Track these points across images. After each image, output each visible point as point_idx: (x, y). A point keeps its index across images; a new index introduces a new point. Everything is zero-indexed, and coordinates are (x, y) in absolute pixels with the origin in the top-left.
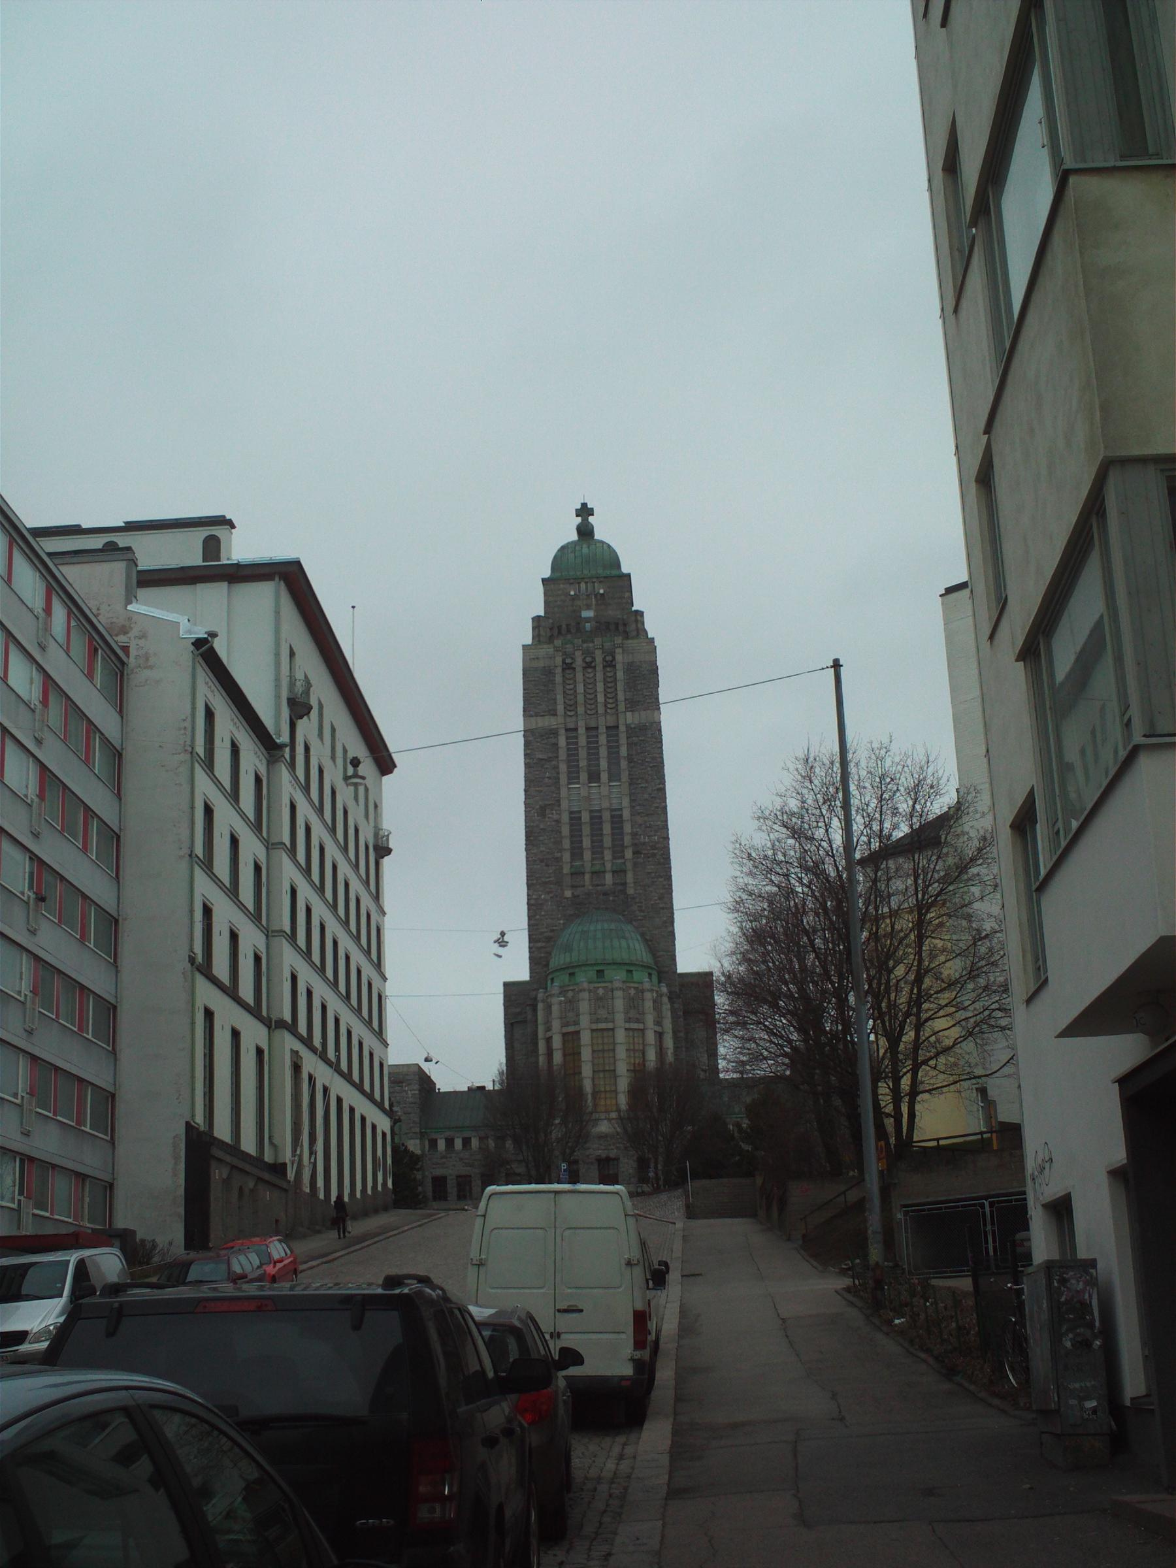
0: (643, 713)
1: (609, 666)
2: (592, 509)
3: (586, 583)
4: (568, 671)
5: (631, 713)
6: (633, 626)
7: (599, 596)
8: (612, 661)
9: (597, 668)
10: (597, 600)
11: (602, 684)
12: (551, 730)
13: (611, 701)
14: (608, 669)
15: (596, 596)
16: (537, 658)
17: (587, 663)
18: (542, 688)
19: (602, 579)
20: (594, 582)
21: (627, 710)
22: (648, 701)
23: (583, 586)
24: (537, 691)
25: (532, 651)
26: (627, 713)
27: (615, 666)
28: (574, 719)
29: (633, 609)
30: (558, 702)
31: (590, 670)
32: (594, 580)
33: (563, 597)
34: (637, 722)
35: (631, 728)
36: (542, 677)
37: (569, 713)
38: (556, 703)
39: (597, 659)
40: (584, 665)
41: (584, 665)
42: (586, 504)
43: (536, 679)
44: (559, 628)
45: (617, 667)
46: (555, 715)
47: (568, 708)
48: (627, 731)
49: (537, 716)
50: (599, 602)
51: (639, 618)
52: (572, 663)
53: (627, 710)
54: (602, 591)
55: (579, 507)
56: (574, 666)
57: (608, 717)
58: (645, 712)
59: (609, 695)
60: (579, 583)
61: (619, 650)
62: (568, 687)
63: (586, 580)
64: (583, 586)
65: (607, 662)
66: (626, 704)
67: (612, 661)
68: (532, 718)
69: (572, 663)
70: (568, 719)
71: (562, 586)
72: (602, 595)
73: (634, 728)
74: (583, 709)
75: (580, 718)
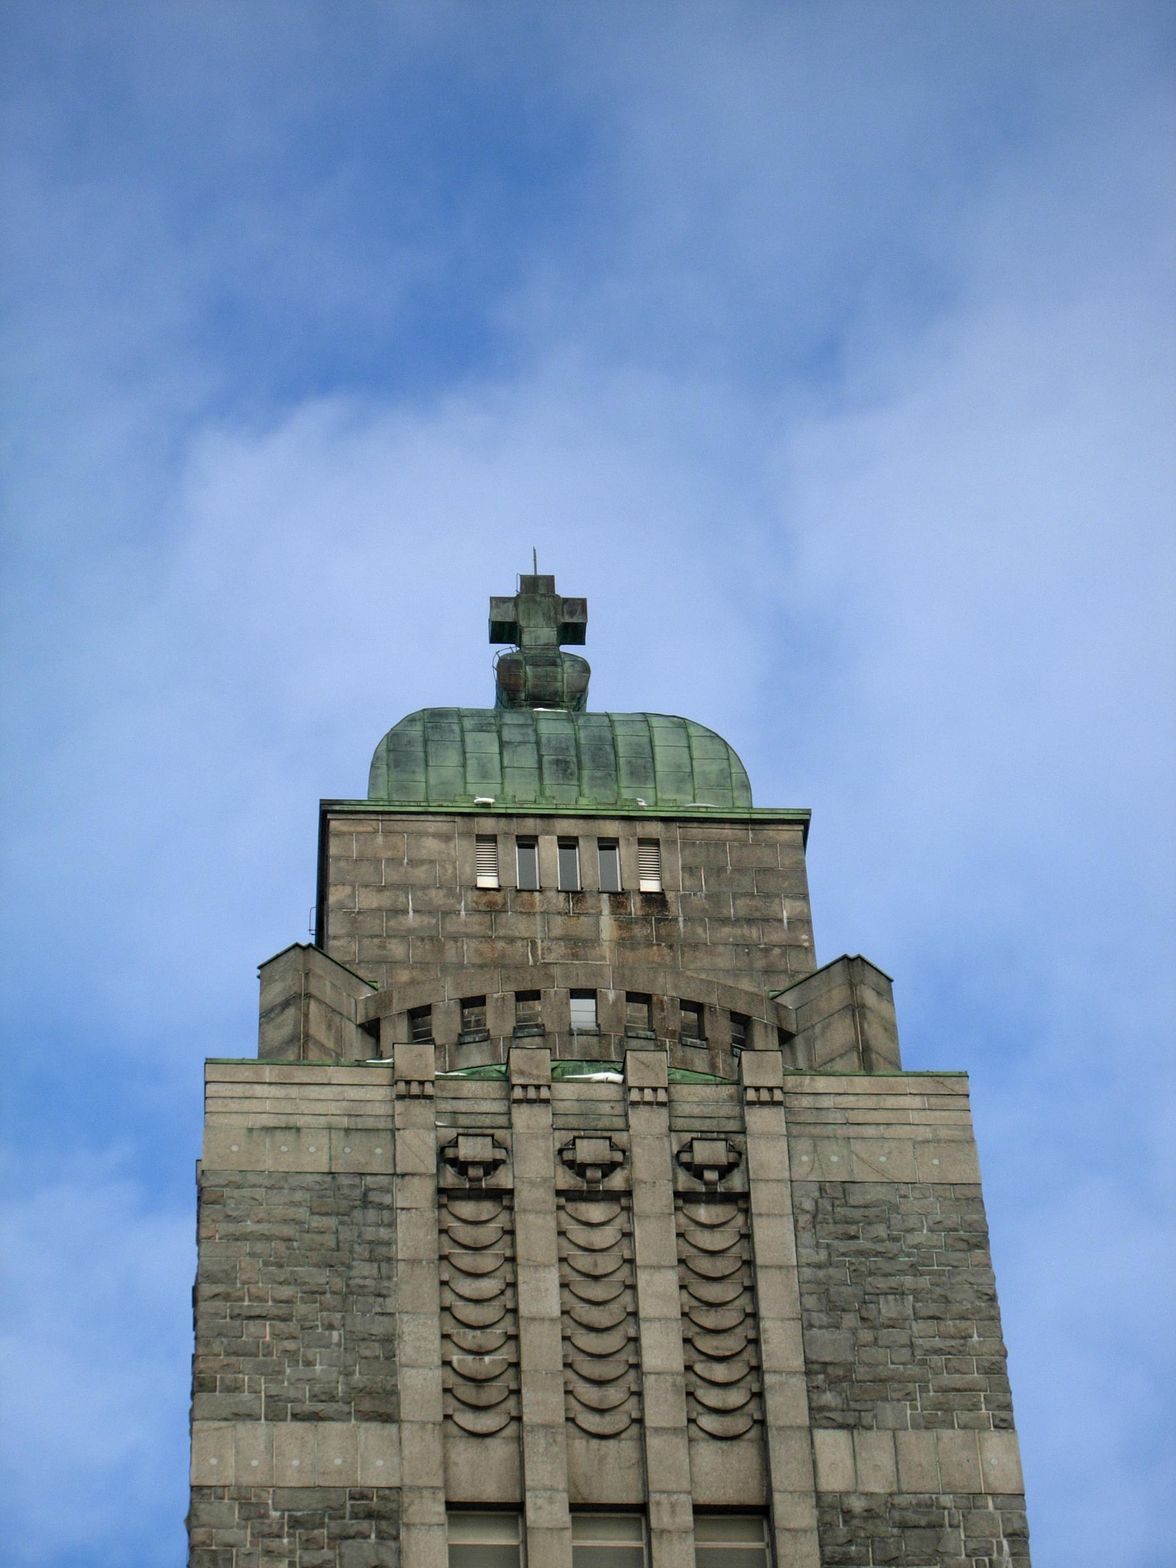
0: (917, 1444)
1: (712, 1197)
2: (580, 605)
3: (568, 843)
4: (467, 1209)
5: (842, 1436)
6: (841, 1033)
7: (635, 906)
8: (725, 1171)
9: (643, 1201)
10: (625, 923)
11: (671, 1278)
12: (360, 1495)
13: (720, 1372)
14: (703, 1213)
15: (619, 898)
16: (298, 1130)
17: (579, 1169)
18: (321, 1277)
19: (654, 830)
20: (608, 844)
21: (819, 1417)
22: (947, 1379)
23: (548, 849)
24: (287, 1292)
25: (259, 1090)
26: (821, 1435)
27: (741, 1200)
28: (499, 1451)
29: (824, 956)
30: (406, 1351)
31: (595, 1212)
32: (611, 829)
33: (437, 897)
34: (878, 1486)
35: (848, 1514)
36: (317, 1222)
37: (468, 1420)
38: (390, 1357)
39: (637, 1151)
40: (566, 1180)
41: (566, 1180)
42: (550, 580)
43: (288, 1231)
44: (419, 1015)
45: (761, 1198)
46: (388, 1418)
47: (467, 1392)
48: (824, 1528)
49: (274, 1416)
50: (639, 931)
51: (869, 997)
52: (492, 1166)
53: (819, 1417)
54: (650, 885)
55: (511, 589)
56: (503, 1179)
57: (707, 1453)
58: (928, 1436)
59: (708, 1345)
60: (527, 842)
61: (761, 1120)
62: (467, 1287)
63: (566, 827)
64: (548, 849)
65: (696, 1171)
66: (811, 1390)
67: (725, 1171)
68: (244, 1429)
69: (492, 1166)
70: (464, 1453)
71: (431, 845)
72: (655, 901)
73: (870, 1514)
74: (557, 1399)
75: (536, 1444)
